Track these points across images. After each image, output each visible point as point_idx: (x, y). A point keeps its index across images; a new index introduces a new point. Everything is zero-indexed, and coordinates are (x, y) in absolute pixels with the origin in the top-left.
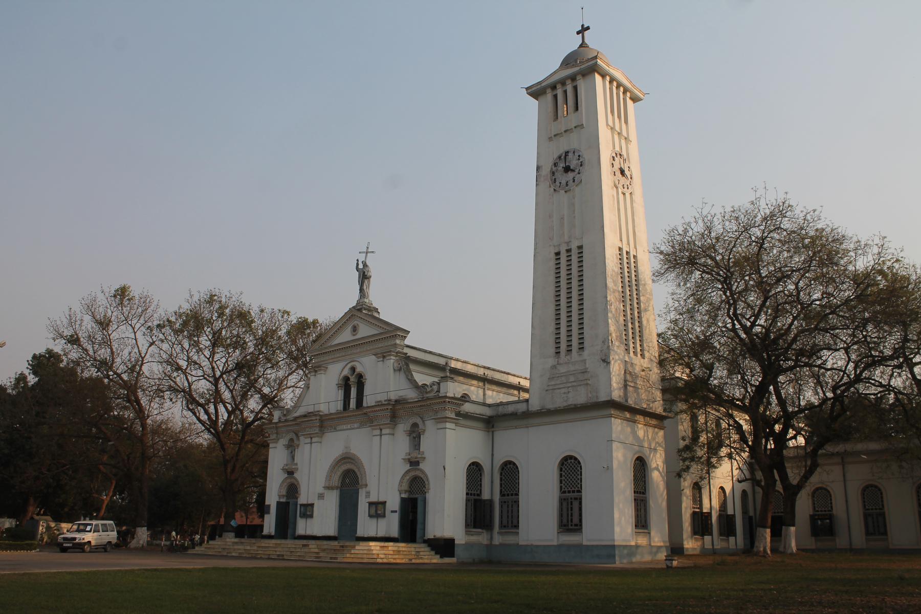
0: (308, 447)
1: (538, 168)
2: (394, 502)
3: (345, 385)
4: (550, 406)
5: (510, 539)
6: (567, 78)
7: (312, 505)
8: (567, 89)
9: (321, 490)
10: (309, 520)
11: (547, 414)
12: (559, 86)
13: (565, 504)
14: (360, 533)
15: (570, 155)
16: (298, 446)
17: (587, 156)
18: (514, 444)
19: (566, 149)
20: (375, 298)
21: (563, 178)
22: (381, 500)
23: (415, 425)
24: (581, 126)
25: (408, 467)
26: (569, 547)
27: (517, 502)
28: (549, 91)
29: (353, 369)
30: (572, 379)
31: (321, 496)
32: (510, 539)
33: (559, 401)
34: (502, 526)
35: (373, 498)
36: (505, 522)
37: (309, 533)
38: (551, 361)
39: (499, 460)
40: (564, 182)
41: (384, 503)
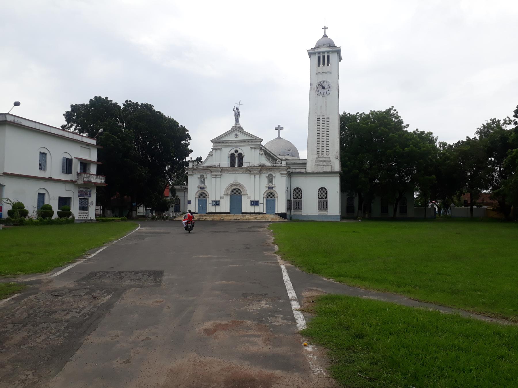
0: (214, 179)
1: (311, 84)
2: (263, 201)
3: (232, 156)
4: (316, 171)
5: (298, 213)
6: (326, 51)
7: (219, 201)
8: (325, 55)
9: (222, 195)
10: (217, 207)
11: (313, 174)
12: (321, 53)
13: (320, 203)
14: (243, 211)
15: (325, 83)
16: (206, 178)
17: (332, 85)
18: (299, 182)
19: (324, 80)
20: (242, 123)
21: (322, 91)
22: (256, 200)
23: (271, 175)
24: (331, 73)
25: (267, 189)
26: (323, 216)
27: (301, 202)
28: (317, 54)
29: (236, 151)
30: (325, 163)
31: (221, 198)
32: (298, 213)
33: (320, 169)
34: (294, 209)
35: (253, 199)
36: (295, 207)
37: (217, 211)
38: (317, 156)
39: (293, 188)
40: (322, 93)
41: (258, 201)
